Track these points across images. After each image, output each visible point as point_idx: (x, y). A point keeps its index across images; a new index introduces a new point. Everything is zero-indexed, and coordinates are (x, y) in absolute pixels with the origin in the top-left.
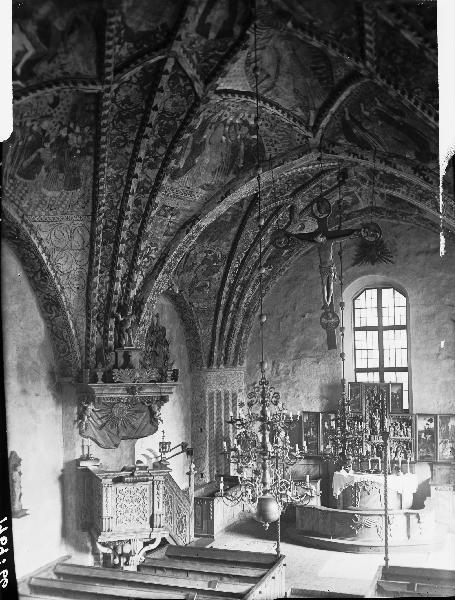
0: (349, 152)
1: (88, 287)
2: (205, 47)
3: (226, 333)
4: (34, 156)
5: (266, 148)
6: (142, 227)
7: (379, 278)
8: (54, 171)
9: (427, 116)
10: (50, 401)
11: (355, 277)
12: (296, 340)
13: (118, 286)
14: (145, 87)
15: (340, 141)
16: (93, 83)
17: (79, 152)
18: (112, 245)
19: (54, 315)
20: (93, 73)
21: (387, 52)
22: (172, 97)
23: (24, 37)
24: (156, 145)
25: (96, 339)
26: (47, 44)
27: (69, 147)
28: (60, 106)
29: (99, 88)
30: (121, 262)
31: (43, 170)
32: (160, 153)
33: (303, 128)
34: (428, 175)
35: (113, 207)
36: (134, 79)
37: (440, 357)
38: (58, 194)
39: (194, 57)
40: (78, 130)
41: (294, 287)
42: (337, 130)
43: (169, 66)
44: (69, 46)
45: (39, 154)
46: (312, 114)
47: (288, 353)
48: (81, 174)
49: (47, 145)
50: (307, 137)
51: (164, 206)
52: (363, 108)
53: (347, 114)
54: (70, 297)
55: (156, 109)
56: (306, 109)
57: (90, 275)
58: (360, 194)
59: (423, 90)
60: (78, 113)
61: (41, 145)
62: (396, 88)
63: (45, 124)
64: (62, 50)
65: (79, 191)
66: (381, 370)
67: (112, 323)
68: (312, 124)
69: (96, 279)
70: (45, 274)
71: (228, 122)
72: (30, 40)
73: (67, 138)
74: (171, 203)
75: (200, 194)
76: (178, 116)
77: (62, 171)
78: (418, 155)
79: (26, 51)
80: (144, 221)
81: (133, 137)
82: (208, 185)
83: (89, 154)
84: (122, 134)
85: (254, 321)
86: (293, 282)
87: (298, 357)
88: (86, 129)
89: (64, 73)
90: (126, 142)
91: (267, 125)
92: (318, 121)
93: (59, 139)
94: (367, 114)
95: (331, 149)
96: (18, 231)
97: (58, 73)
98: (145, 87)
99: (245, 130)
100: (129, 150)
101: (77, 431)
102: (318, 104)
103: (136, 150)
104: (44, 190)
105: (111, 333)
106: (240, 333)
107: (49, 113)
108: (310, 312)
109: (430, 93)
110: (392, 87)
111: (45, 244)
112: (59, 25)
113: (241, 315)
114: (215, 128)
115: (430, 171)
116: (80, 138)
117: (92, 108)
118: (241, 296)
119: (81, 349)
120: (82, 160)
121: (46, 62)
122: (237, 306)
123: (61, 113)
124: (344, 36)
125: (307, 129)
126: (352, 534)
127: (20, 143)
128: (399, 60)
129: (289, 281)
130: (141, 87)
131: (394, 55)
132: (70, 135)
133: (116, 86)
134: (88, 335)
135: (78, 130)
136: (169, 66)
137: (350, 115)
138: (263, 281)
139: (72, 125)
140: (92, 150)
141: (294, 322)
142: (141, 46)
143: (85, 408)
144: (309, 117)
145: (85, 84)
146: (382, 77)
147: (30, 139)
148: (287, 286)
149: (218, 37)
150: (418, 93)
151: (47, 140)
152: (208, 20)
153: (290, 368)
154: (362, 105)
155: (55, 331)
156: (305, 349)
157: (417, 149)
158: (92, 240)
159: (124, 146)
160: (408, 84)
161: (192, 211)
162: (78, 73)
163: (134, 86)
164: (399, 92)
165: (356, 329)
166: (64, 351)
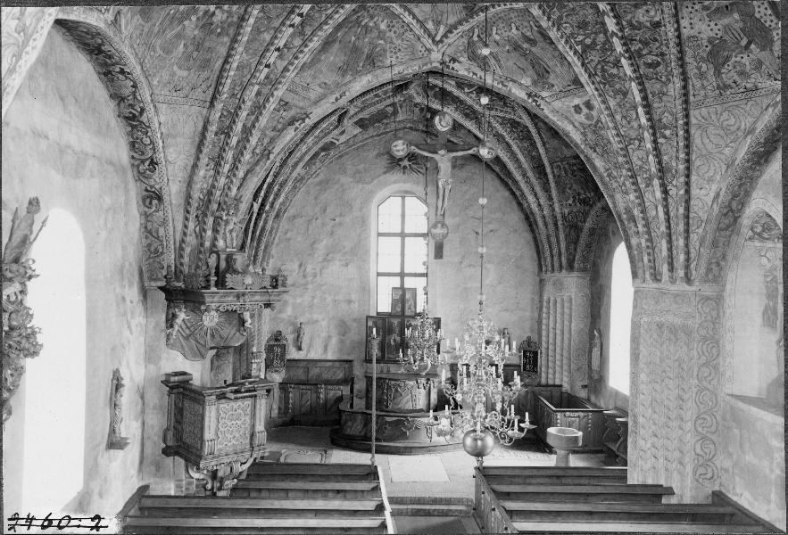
0: (468, 70)
1: (190, 184)
3: (258, 233)
4: (180, 27)
5: (388, 55)
6: (257, 119)
7: (407, 186)
8: (191, 48)
9: (568, 50)
10: (139, 308)
11: (386, 184)
12: (324, 242)
13: (222, 181)
15: (461, 59)
17: (219, 30)
18: (223, 136)
19: (152, 210)
24: (293, 36)
25: (191, 240)
30: (229, 156)
31: (182, 46)
32: (296, 44)
33: (430, 41)
34: (540, 101)
35: (234, 95)
37: (463, 266)
38: (185, 73)
41: (325, 190)
42: (461, 48)
45: (184, 25)
46: (442, 30)
47: (316, 255)
49: (194, 18)
50: (429, 51)
51: (281, 100)
52: (494, 32)
53: (476, 35)
54: (174, 193)
56: (438, 23)
57: (195, 166)
58: (401, 107)
62: (549, 19)
65: (205, 74)
66: (402, 275)
67: (210, 221)
68: (438, 38)
69: (202, 173)
70: (153, 163)
71: (363, 23)
73: (214, 14)
74: (289, 98)
75: (316, 91)
77: (197, 50)
78: (535, 83)
80: (261, 113)
81: (276, 24)
82: (325, 83)
83: (227, 34)
84: (269, 17)
85: (284, 223)
86: (325, 184)
87: (326, 260)
90: (267, 30)
91: (395, 32)
92: (445, 36)
94: (497, 38)
95: (451, 65)
96: (143, 110)
99: (375, 33)
100: (267, 37)
101: (164, 340)
102: (452, 20)
104: (175, 68)
105: (209, 233)
106: (271, 232)
108: (341, 215)
109: (576, 29)
110: (546, 18)
111: (163, 130)
113: (273, 214)
114: (351, 28)
115: (543, 98)
116: (226, 15)
118: (277, 195)
119: (175, 248)
120: (220, 40)
122: (272, 206)
125: (433, 40)
126: (403, 436)
129: (320, 183)
132: (217, 12)
134: (185, 234)
137: (478, 36)
138: (300, 179)
140: (232, 31)
141: (323, 225)
143: (174, 316)
144: (437, 30)
148: (318, 188)
150: (565, 28)
153: (318, 270)
154: (495, 28)
155: (149, 227)
156: (333, 252)
157: (536, 77)
158: (205, 128)
160: (560, 18)
161: (302, 108)
164: (550, 23)
165: (379, 235)
166: (156, 251)
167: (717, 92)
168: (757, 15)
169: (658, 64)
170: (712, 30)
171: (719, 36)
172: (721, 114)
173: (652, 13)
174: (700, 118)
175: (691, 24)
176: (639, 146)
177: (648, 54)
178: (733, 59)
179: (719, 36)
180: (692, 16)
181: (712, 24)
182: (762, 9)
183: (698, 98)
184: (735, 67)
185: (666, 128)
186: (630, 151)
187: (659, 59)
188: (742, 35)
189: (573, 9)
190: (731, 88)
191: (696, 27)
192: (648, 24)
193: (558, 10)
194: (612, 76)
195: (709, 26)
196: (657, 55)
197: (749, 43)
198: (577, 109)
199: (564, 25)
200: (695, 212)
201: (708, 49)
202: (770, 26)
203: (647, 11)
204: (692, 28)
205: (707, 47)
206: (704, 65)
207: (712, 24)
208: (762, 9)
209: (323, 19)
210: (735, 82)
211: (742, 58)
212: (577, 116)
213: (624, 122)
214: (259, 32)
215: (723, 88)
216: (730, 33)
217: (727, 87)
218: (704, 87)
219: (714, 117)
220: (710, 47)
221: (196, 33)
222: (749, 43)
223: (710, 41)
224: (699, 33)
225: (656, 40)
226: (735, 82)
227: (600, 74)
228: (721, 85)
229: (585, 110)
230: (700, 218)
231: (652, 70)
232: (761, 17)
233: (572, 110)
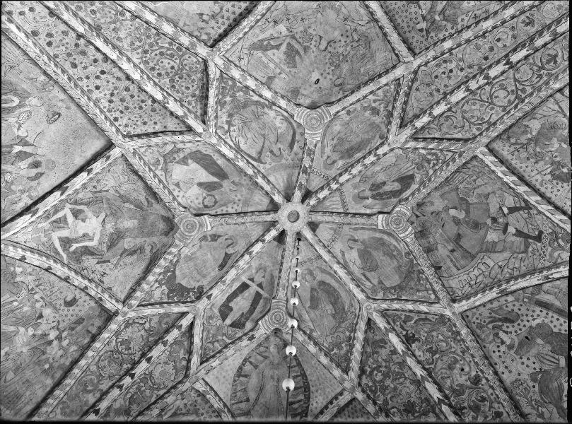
2: (218, 329)
14: (151, 339)
16: (117, 301)
20: (122, 297)
21: (369, 370)
22: (166, 363)
23: (100, 228)
26: (109, 248)
27: (44, 353)
28: (71, 308)
29: (120, 306)
36: (147, 326)
39: (205, 333)
40: (65, 343)
43: (185, 323)
44: (121, 263)
48: (28, 393)
55: (149, 360)
59: (399, 410)
60: (79, 328)
61: (26, 325)
63: (47, 312)
64: (115, 262)
72: (102, 235)
73: (50, 343)
76: (158, 389)
79: (91, 239)
83: (53, 377)
88: (74, 348)
89: (100, 281)
93: (45, 335)
97: (96, 277)
98: (151, 339)
103: (100, 400)
107: (58, 306)
112: (127, 243)
116: (61, 352)
117: (94, 330)
120: (43, 378)
121: (96, 261)
123: (66, 316)
124: (335, 350)
127: (15, 304)
128: (379, 377)
130: (148, 338)
131: (375, 372)
132: (55, 343)
133: (132, 314)
135: (65, 343)
136: (185, 323)
139: (64, 334)
140: (58, 375)
142: (173, 297)
145: (110, 297)
146: (363, 391)
147: (26, 309)
149: (232, 325)
151: (36, 326)
152: (232, 304)
159: (90, 392)
160: (386, 402)
162: (110, 288)
163: (143, 332)
168: (555, 330)
170: (528, 366)
171: (538, 370)
173: (467, 369)
179: (538, 370)
180: (503, 359)
181: (524, 359)
182: (556, 323)
188: (557, 357)
189: (395, 389)
192: (469, 383)
193: (381, 393)
195: (523, 363)
199: (392, 411)
203: (462, 370)
204: (510, 372)
205: (534, 387)
206: (544, 410)
207: (524, 359)
208: (556, 323)
209: (153, 400)
214: (86, 391)
216: (545, 361)
220: (537, 386)
221: (25, 350)
224: (519, 374)
225: (483, 399)
232: (560, 330)
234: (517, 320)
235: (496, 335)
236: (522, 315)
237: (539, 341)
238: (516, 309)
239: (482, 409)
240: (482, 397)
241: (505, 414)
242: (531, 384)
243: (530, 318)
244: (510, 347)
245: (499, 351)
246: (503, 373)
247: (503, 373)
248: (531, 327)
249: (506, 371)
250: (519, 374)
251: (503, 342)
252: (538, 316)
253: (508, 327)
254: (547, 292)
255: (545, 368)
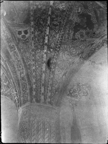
167: (72, 40)
169: (57, 25)
171: (78, 23)
172: (71, 48)
174: (63, 48)
175: (73, 16)
176: (40, 52)
177: (56, 21)
178: (80, 31)
183: (65, 41)
184: (80, 33)
185: (52, 48)
186: (37, 53)
187: (58, 24)
188: (85, 24)
190: (77, 40)
191: (74, 17)
192: (61, 10)
194: (40, 24)
195: (77, 18)
196: (58, 22)
197: (87, 27)
198: (20, 33)
200: (55, 79)
201: (74, 26)
202: (94, 23)
204: (72, 17)
205: (74, 25)
210: (78, 38)
211: (83, 31)
212: (18, 36)
213: (38, 42)
215: (74, 39)
217: (75, 39)
218: (68, 38)
219: (68, 49)
222: (87, 27)
223: (76, 23)
225: (61, 16)
226: (78, 38)
227: (36, 21)
228: (74, 38)
229: (23, 34)
230: (57, 81)
231: (54, 27)
232: (92, 20)
233: (17, 32)
234: (87, 9)
235: (79, 7)
236: (89, 9)
237: (85, 18)
238: (89, 6)
239: (58, 18)
240: (61, 16)
241: (62, 24)
242: (74, 24)
243: (89, 12)
244: (78, 13)
245: (75, 11)
246: (71, 16)
247: (71, 16)
248: (87, 13)
249: (72, 16)
250: (74, 20)
251: (78, 10)
252: (92, 13)
253: (83, 8)
254: (99, 11)
255: (81, 24)
